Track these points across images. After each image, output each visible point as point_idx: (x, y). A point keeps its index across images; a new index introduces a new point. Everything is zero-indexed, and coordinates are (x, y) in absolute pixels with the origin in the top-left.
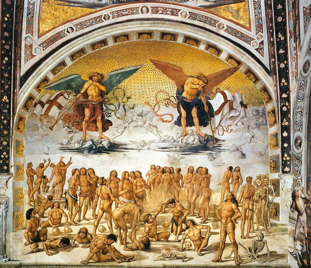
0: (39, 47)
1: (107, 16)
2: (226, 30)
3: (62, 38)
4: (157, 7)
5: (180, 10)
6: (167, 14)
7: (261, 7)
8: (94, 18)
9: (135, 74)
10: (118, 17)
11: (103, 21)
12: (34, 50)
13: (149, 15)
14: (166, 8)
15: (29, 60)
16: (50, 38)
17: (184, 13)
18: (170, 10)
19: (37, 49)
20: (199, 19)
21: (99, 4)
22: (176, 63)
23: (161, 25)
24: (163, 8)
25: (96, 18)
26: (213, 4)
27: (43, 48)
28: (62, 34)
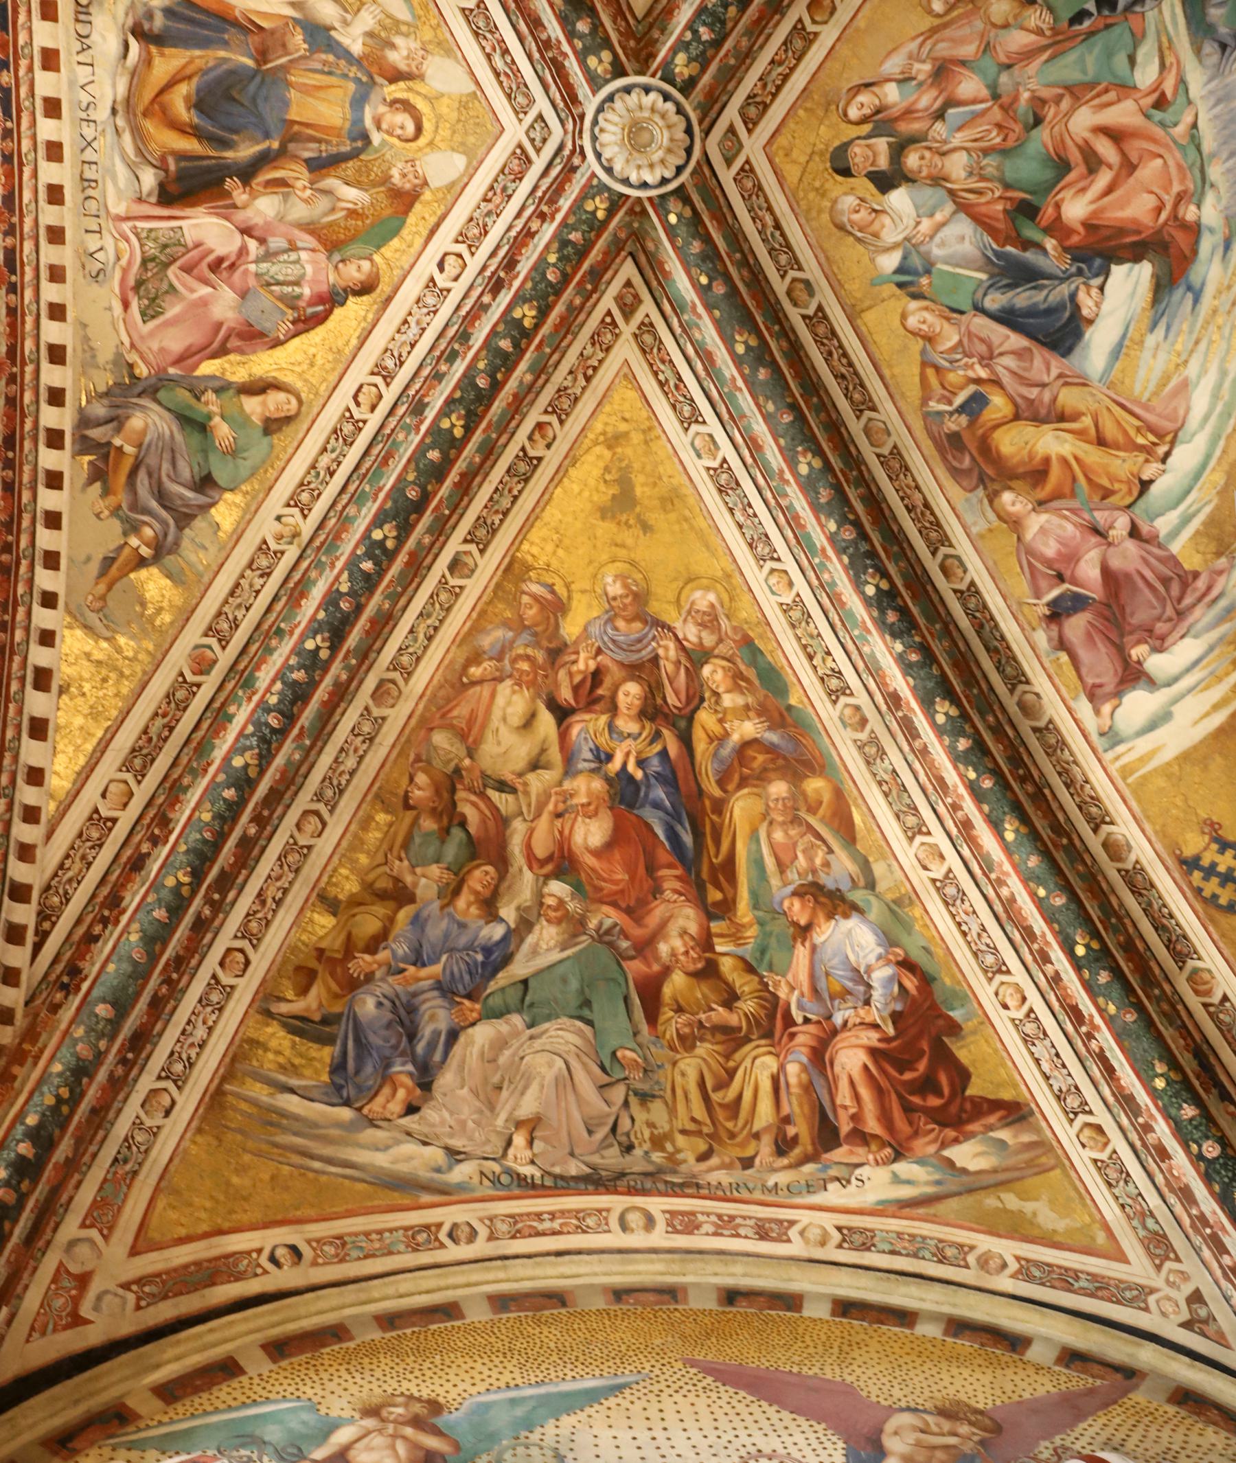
0: (120, 1291)
1: (467, 1229)
2: (1019, 1272)
3: (237, 1279)
4: (693, 1214)
5: (792, 1223)
6: (738, 1235)
7: (1128, 1175)
8: (406, 1229)
9: (612, 1401)
10: (514, 1237)
11: (442, 1246)
12: (91, 1294)
13: (659, 1238)
14: (732, 1218)
15: (55, 1330)
16: (186, 1266)
17: (814, 1234)
18: (752, 1222)
19: (108, 1298)
20: (887, 1247)
21: (432, 1180)
22: (816, 1370)
23: (719, 1268)
24: (720, 1217)
25: (411, 1232)
26: (930, 1190)
27: (139, 1299)
28: (245, 1262)
